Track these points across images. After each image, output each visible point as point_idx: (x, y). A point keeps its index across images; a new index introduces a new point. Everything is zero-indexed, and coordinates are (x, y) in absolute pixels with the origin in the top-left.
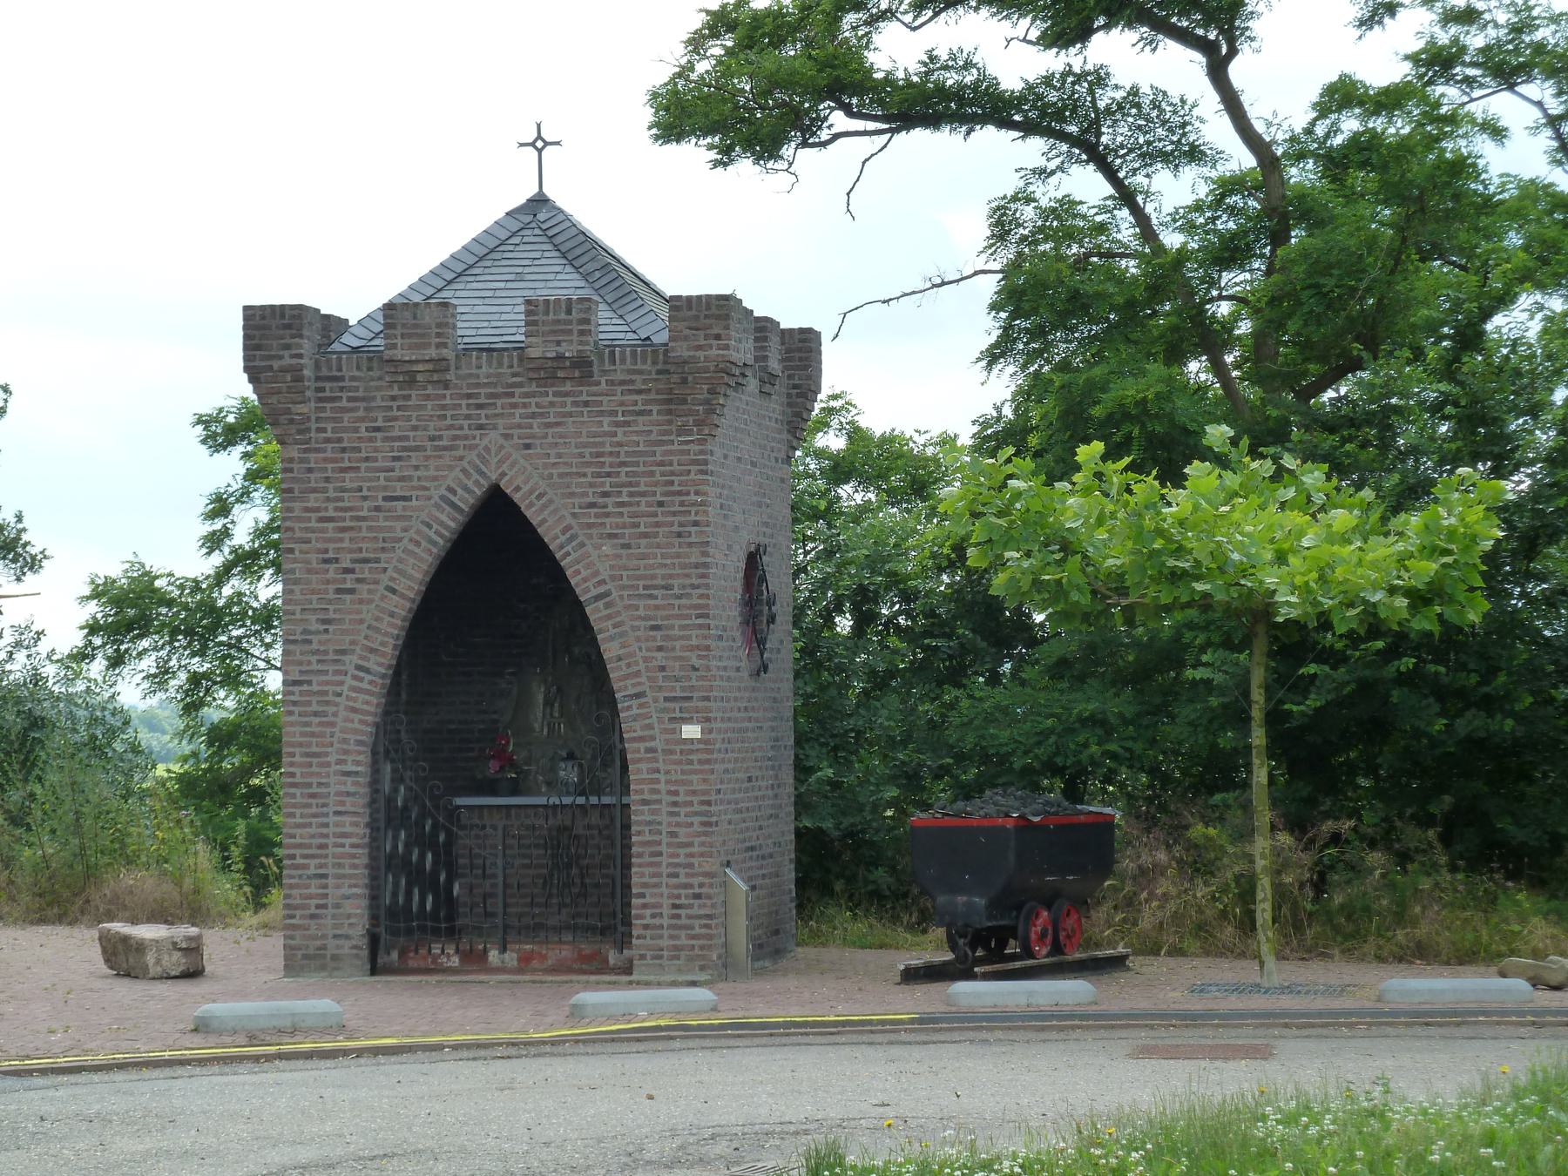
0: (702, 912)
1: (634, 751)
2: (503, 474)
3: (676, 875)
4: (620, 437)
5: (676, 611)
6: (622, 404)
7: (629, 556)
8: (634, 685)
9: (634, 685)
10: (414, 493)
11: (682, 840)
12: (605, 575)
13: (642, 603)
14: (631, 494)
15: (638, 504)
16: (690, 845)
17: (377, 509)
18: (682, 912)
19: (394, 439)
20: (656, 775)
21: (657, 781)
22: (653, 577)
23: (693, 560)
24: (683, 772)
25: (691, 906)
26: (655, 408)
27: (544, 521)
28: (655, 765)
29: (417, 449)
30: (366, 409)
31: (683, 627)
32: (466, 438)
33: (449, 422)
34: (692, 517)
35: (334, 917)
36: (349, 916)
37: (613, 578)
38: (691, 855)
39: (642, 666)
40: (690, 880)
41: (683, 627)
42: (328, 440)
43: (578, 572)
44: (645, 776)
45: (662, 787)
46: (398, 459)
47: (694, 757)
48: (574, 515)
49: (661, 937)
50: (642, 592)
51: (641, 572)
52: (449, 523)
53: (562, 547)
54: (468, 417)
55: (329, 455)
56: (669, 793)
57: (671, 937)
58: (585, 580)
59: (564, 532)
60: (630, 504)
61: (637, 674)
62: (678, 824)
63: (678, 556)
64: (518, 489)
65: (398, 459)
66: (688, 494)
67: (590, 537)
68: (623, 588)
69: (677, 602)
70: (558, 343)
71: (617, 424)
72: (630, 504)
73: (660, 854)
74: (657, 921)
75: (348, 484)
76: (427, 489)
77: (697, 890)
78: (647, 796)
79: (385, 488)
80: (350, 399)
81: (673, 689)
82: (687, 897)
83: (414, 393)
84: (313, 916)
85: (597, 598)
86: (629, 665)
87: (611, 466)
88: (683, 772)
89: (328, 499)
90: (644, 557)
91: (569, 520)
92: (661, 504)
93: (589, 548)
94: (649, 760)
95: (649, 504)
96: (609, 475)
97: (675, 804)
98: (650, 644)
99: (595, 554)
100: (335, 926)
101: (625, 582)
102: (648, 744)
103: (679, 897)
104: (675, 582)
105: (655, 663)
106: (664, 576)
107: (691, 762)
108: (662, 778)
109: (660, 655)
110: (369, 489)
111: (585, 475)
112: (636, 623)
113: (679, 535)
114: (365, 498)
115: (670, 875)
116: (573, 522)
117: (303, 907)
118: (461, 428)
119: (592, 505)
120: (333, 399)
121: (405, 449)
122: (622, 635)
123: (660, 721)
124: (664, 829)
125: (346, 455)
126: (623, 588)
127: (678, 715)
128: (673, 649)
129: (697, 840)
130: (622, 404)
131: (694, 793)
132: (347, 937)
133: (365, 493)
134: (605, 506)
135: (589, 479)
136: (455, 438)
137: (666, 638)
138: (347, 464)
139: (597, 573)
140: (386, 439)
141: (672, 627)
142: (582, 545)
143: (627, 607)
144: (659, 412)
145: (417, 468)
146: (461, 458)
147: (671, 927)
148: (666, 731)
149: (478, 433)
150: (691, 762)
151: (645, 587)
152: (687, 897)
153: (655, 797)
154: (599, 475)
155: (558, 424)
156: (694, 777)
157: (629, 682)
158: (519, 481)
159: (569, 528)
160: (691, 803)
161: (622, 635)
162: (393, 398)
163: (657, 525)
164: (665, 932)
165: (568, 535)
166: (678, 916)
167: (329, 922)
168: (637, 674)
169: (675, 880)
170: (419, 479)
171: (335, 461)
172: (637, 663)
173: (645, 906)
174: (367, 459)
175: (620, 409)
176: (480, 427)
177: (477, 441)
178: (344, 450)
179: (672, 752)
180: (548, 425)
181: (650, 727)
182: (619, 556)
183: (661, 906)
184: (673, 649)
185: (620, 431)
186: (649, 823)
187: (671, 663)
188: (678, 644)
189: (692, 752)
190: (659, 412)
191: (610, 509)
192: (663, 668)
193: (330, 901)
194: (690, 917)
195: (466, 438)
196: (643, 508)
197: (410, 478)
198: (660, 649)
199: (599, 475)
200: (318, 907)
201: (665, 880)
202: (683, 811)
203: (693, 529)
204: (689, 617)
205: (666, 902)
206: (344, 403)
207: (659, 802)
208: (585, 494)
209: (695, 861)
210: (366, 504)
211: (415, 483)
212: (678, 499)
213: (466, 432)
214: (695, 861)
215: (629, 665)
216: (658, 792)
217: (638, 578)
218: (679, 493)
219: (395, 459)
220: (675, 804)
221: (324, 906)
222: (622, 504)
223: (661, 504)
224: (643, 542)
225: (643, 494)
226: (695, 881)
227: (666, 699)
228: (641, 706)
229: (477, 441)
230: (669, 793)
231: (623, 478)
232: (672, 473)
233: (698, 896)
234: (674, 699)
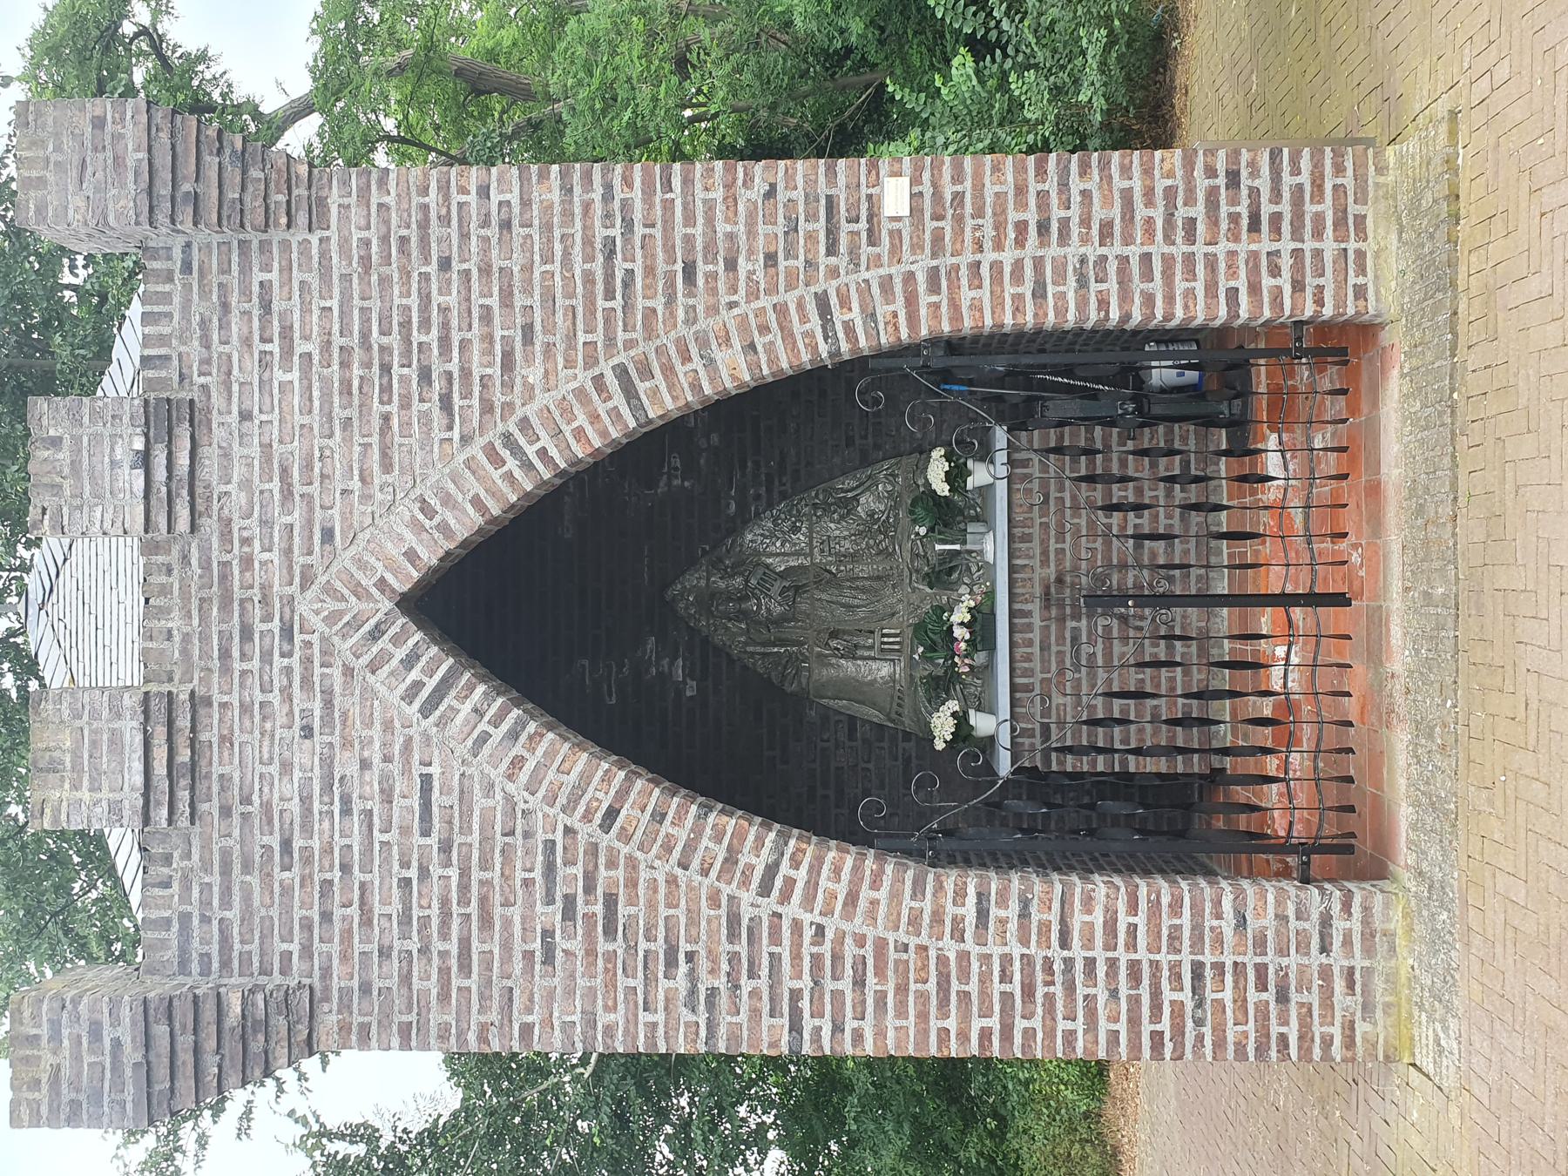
0: (1265, 170)
1: (934, 320)
2: (382, 584)
3: (1191, 223)
4: (312, 347)
5: (657, 232)
6: (247, 342)
7: (549, 329)
8: (804, 319)
9: (804, 319)
10: (417, 769)
11: (1116, 213)
12: (584, 378)
13: (640, 303)
14: (425, 324)
15: (444, 310)
16: (1127, 195)
17: (446, 847)
18: (1266, 210)
19: (307, 811)
20: (985, 271)
21: (996, 267)
22: (589, 279)
23: (556, 196)
24: (979, 213)
25: (1254, 193)
26: (258, 276)
27: (476, 502)
28: (964, 272)
29: (328, 763)
30: (247, 867)
31: (690, 220)
32: (307, 661)
33: (275, 698)
34: (472, 198)
35: (1283, 951)
36: (1282, 918)
37: (591, 361)
38: (1149, 193)
39: (765, 302)
40: (1201, 196)
41: (690, 220)
42: (307, 951)
43: (579, 433)
44: (985, 294)
45: (1008, 257)
46: (346, 801)
47: (948, 192)
48: (466, 440)
49: (1318, 254)
50: (618, 303)
51: (579, 303)
52: (475, 702)
53: (528, 466)
54: (266, 657)
55: (335, 948)
56: (1020, 242)
57: (1318, 234)
58: (594, 418)
59: (498, 462)
60: (445, 326)
61: (781, 310)
62: (1086, 222)
63: (547, 227)
64: (411, 555)
65: (346, 801)
66: (425, 208)
67: (508, 407)
68: (610, 341)
69: (639, 230)
70: (114, 464)
71: (287, 352)
72: (445, 326)
73: (1146, 258)
74: (1286, 262)
75: (395, 908)
76: (408, 741)
77: (1221, 181)
78: (1027, 289)
79: (405, 831)
80: (226, 903)
81: (811, 237)
82: (1234, 202)
83: (216, 770)
84: (1282, 997)
85: (630, 393)
86: (764, 329)
87: (368, 365)
88: (979, 213)
89: (424, 951)
90: (549, 298)
91: (476, 450)
92: (445, 264)
93: (531, 410)
94: (954, 286)
95: (445, 290)
96: (386, 369)
97: (1043, 228)
98: (721, 286)
99: (542, 399)
100: (1302, 947)
101: (599, 337)
102: (922, 287)
103: (1234, 218)
104: (600, 233)
105: (760, 275)
106: (589, 258)
107: (958, 197)
108: (989, 256)
109: (743, 265)
110: (405, 865)
111: (386, 418)
112: (681, 314)
113: (506, 225)
114: (424, 873)
115: (1190, 238)
116: (480, 442)
117: (1263, 1012)
118: (288, 671)
119: (446, 403)
120: (225, 940)
121: (327, 788)
122: (703, 343)
123: (876, 261)
124: (1093, 251)
125: (338, 913)
126: (610, 341)
127: (863, 225)
128: (731, 236)
129: (1119, 183)
130: (247, 342)
131: (1021, 190)
132: (1326, 921)
133: (413, 873)
134: (449, 375)
135: (394, 408)
136: (306, 682)
137: (710, 251)
138: (354, 911)
139: (580, 393)
140: (307, 829)
141: (689, 240)
142: (524, 424)
143: (650, 332)
144: (267, 268)
145: (365, 765)
146: (348, 671)
147: (1297, 235)
148: (895, 250)
149: (298, 638)
150: (958, 197)
151: (609, 295)
152: (1234, 202)
153: (1029, 272)
154: (386, 389)
155: (285, 471)
156: (990, 191)
157: (797, 328)
158: (394, 551)
159: (490, 452)
160: (1042, 196)
161: (703, 343)
162: (226, 811)
163: (486, 270)
164: (1309, 245)
165: (505, 454)
166: (1276, 219)
167: (1293, 960)
168: (781, 310)
169: (1201, 228)
170: (387, 759)
171: (347, 935)
172: (761, 312)
173: (1254, 289)
174: (346, 868)
175: (258, 346)
176: (287, 633)
177: (315, 638)
178: (326, 917)
179: (938, 237)
180: (287, 493)
181: (886, 284)
182: (548, 348)
183: (1254, 255)
184: (731, 236)
185: (301, 347)
186: (1082, 282)
187: (761, 242)
188: (722, 228)
189: (937, 195)
190: (267, 268)
191: (454, 367)
192: (771, 259)
193: (1250, 960)
194: (1276, 196)
195: (307, 661)
196: (452, 300)
197: (385, 778)
198: (731, 265)
199: (386, 389)
200: (1262, 986)
201: (1200, 249)
202: (1057, 213)
203: (495, 197)
204: (668, 205)
205: (1244, 247)
206: (233, 915)
207: (1038, 263)
208: (425, 418)
209: (1160, 185)
210: (436, 871)
211: (395, 768)
212: (435, 230)
213: (295, 661)
214: (1160, 185)
215: (764, 329)
216: (1018, 265)
217: (591, 310)
218: (424, 225)
219: (346, 811)
220: (1043, 228)
221: (1261, 970)
222: (445, 341)
223: (445, 264)
224: (519, 300)
225: (426, 299)
226: (1202, 183)
227: (832, 250)
228: (845, 303)
229: (315, 638)
230: (1020, 242)
231: (394, 340)
232: (385, 239)
233: (1233, 178)
234: (832, 233)
